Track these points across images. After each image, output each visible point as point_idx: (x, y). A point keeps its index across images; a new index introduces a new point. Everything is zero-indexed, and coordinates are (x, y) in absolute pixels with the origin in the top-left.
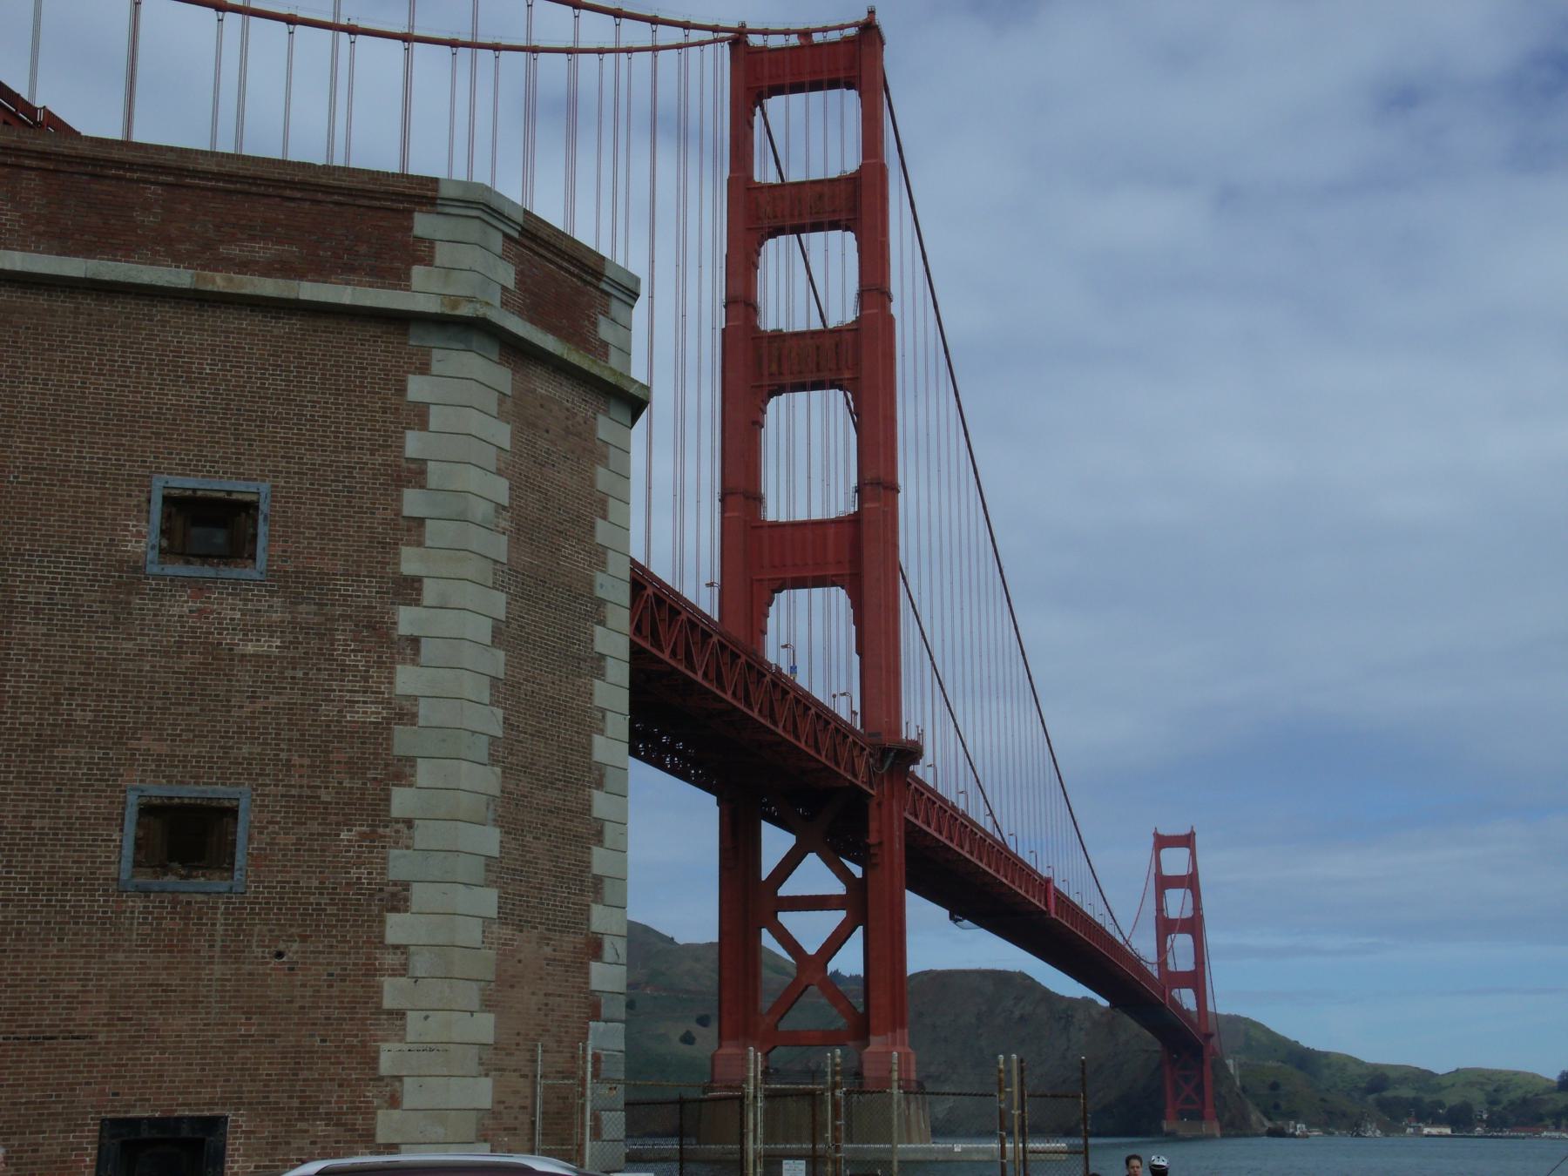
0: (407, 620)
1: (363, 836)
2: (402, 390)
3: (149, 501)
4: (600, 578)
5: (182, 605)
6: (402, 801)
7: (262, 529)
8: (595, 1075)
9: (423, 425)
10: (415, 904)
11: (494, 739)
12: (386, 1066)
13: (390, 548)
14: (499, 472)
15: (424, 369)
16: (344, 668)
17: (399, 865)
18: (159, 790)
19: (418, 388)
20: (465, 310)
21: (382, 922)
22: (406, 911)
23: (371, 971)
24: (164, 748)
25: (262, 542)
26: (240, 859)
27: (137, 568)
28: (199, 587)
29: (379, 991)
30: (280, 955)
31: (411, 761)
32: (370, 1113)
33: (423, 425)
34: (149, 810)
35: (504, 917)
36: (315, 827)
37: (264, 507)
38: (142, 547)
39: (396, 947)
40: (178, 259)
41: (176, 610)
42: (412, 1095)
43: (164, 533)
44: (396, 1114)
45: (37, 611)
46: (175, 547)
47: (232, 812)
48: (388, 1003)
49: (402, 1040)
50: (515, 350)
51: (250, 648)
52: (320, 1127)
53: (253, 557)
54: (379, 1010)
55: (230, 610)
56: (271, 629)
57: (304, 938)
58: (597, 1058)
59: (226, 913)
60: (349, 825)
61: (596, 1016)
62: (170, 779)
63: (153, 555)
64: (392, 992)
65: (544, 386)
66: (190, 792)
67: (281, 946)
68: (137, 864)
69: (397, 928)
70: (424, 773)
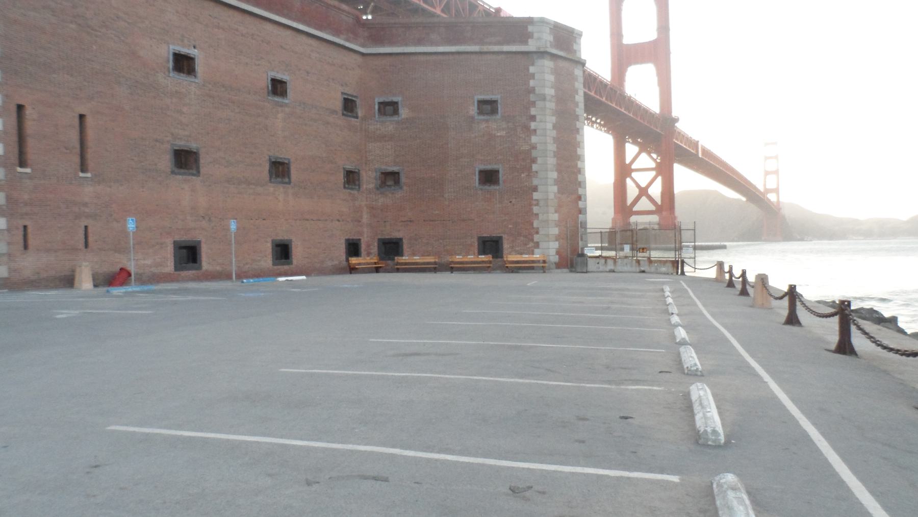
0: (533, 125)
1: (527, 175)
2: (528, 70)
3: (474, 102)
4: (577, 109)
5: (483, 126)
6: (535, 167)
7: (499, 106)
8: (581, 226)
9: (534, 78)
10: (539, 190)
11: (554, 152)
12: (535, 225)
13: (528, 109)
14: (552, 87)
15: (533, 64)
16: (520, 137)
17: (535, 182)
18: (482, 167)
19: (532, 69)
20: (542, 50)
21: (532, 194)
22: (537, 192)
23: (531, 205)
24: (482, 158)
25: (499, 109)
26: (501, 182)
27: (473, 118)
28: (487, 121)
29: (533, 209)
30: (511, 202)
31: (536, 158)
32: (532, 236)
33: (534, 78)
34: (481, 172)
35: (559, 192)
36: (516, 174)
37: (499, 101)
38: (473, 113)
39: (535, 200)
40: (476, 44)
41: (482, 127)
42: (542, 232)
43: (478, 109)
44: (538, 235)
45: (453, 129)
46: (481, 112)
47: (497, 172)
48: (535, 212)
49: (538, 220)
50: (554, 57)
51: (499, 134)
52: (522, 238)
53: (497, 113)
54: (533, 213)
55: (494, 126)
56: (503, 129)
57: (516, 198)
58: (581, 223)
59: (499, 193)
60: (523, 173)
61: (580, 213)
62: (484, 165)
63: (476, 114)
64: (535, 209)
65: (562, 64)
66: (489, 167)
67: (511, 200)
68: (479, 183)
69: (536, 196)
70: (539, 160)
